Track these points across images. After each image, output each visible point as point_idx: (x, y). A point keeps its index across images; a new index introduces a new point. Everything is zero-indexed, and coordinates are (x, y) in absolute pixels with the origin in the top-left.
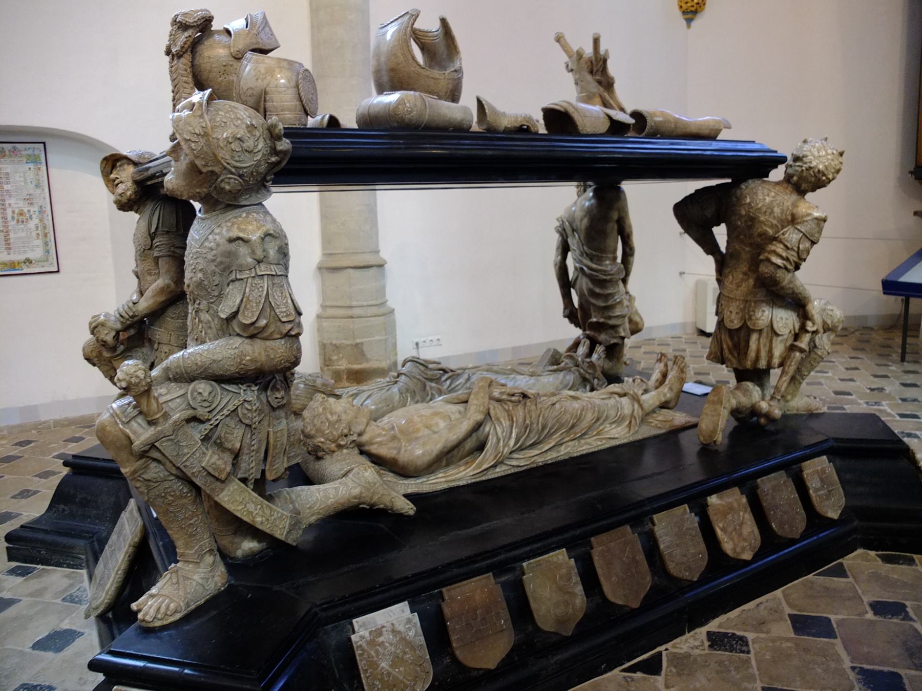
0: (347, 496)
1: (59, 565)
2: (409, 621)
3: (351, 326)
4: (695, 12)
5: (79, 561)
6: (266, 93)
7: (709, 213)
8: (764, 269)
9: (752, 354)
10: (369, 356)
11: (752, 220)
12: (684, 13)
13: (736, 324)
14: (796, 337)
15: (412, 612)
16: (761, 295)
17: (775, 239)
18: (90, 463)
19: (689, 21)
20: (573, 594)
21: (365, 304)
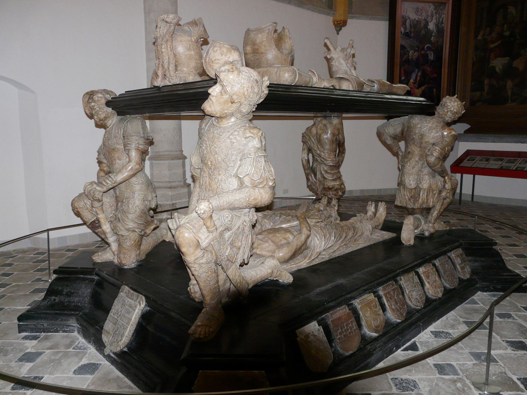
0: (266, 273)
2: (319, 330)
5: (72, 328)
10: (270, 201)
15: (319, 326)
20: (379, 315)
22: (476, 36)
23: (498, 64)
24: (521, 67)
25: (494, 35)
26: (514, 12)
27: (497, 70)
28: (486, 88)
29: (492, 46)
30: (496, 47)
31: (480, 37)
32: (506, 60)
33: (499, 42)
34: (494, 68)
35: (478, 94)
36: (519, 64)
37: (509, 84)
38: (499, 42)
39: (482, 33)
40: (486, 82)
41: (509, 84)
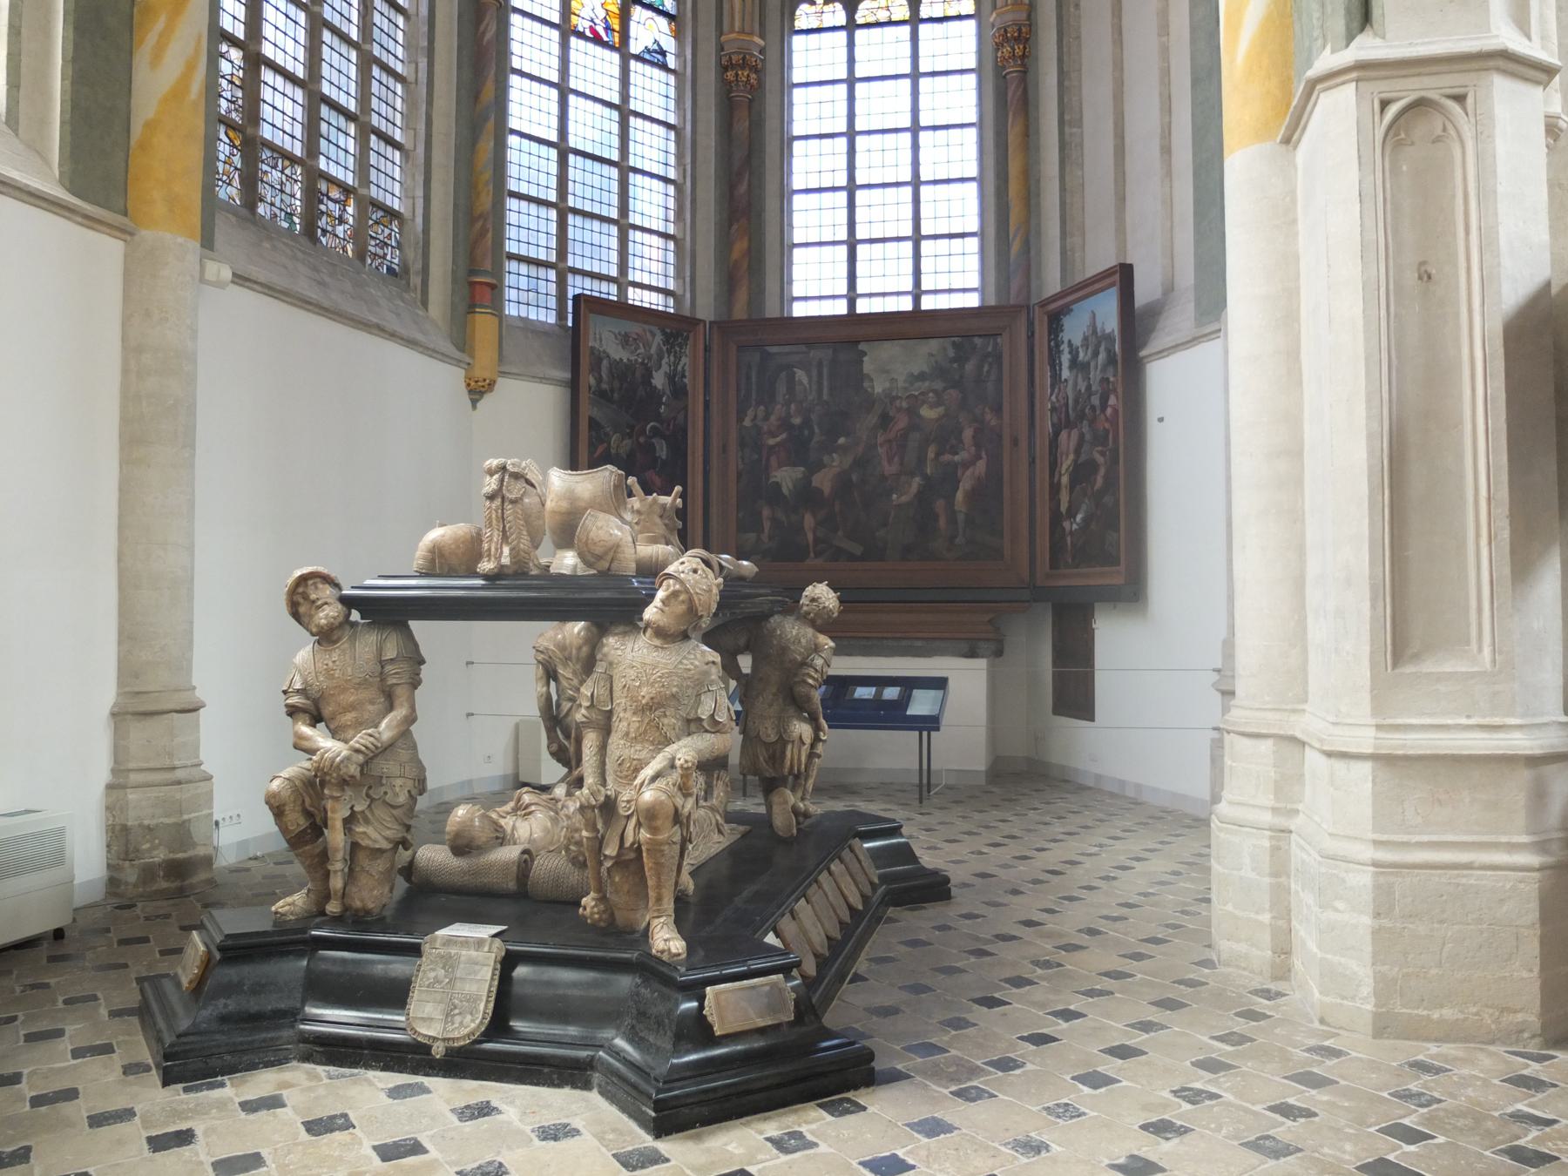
1: (252, 1067)
3: (178, 796)
4: (482, 394)
6: (618, 546)
7: (742, 641)
8: (802, 689)
9: (788, 763)
11: (784, 650)
12: (470, 392)
13: (773, 738)
14: (813, 746)
16: (791, 710)
17: (804, 664)
18: (255, 940)
19: (474, 403)
21: (189, 763)
22: (740, 419)
23: (786, 477)
24: (827, 489)
25: (773, 418)
26: (805, 381)
27: (785, 491)
28: (767, 525)
29: (771, 442)
30: (777, 444)
31: (747, 423)
32: (799, 471)
33: (784, 436)
34: (778, 485)
35: (752, 536)
36: (824, 481)
37: (809, 521)
38: (784, 436)
39: (750, 413)
40: (766, 512)
41: (809, 521)
